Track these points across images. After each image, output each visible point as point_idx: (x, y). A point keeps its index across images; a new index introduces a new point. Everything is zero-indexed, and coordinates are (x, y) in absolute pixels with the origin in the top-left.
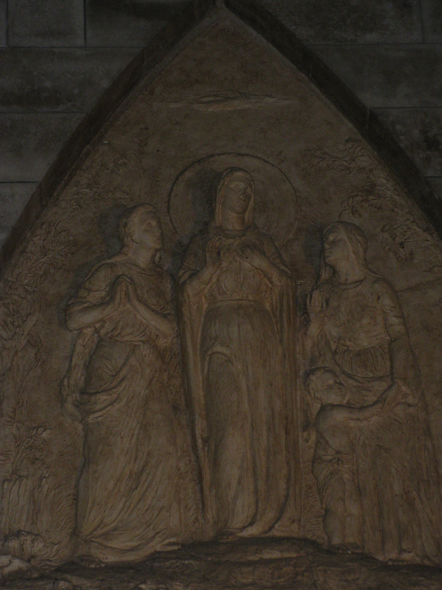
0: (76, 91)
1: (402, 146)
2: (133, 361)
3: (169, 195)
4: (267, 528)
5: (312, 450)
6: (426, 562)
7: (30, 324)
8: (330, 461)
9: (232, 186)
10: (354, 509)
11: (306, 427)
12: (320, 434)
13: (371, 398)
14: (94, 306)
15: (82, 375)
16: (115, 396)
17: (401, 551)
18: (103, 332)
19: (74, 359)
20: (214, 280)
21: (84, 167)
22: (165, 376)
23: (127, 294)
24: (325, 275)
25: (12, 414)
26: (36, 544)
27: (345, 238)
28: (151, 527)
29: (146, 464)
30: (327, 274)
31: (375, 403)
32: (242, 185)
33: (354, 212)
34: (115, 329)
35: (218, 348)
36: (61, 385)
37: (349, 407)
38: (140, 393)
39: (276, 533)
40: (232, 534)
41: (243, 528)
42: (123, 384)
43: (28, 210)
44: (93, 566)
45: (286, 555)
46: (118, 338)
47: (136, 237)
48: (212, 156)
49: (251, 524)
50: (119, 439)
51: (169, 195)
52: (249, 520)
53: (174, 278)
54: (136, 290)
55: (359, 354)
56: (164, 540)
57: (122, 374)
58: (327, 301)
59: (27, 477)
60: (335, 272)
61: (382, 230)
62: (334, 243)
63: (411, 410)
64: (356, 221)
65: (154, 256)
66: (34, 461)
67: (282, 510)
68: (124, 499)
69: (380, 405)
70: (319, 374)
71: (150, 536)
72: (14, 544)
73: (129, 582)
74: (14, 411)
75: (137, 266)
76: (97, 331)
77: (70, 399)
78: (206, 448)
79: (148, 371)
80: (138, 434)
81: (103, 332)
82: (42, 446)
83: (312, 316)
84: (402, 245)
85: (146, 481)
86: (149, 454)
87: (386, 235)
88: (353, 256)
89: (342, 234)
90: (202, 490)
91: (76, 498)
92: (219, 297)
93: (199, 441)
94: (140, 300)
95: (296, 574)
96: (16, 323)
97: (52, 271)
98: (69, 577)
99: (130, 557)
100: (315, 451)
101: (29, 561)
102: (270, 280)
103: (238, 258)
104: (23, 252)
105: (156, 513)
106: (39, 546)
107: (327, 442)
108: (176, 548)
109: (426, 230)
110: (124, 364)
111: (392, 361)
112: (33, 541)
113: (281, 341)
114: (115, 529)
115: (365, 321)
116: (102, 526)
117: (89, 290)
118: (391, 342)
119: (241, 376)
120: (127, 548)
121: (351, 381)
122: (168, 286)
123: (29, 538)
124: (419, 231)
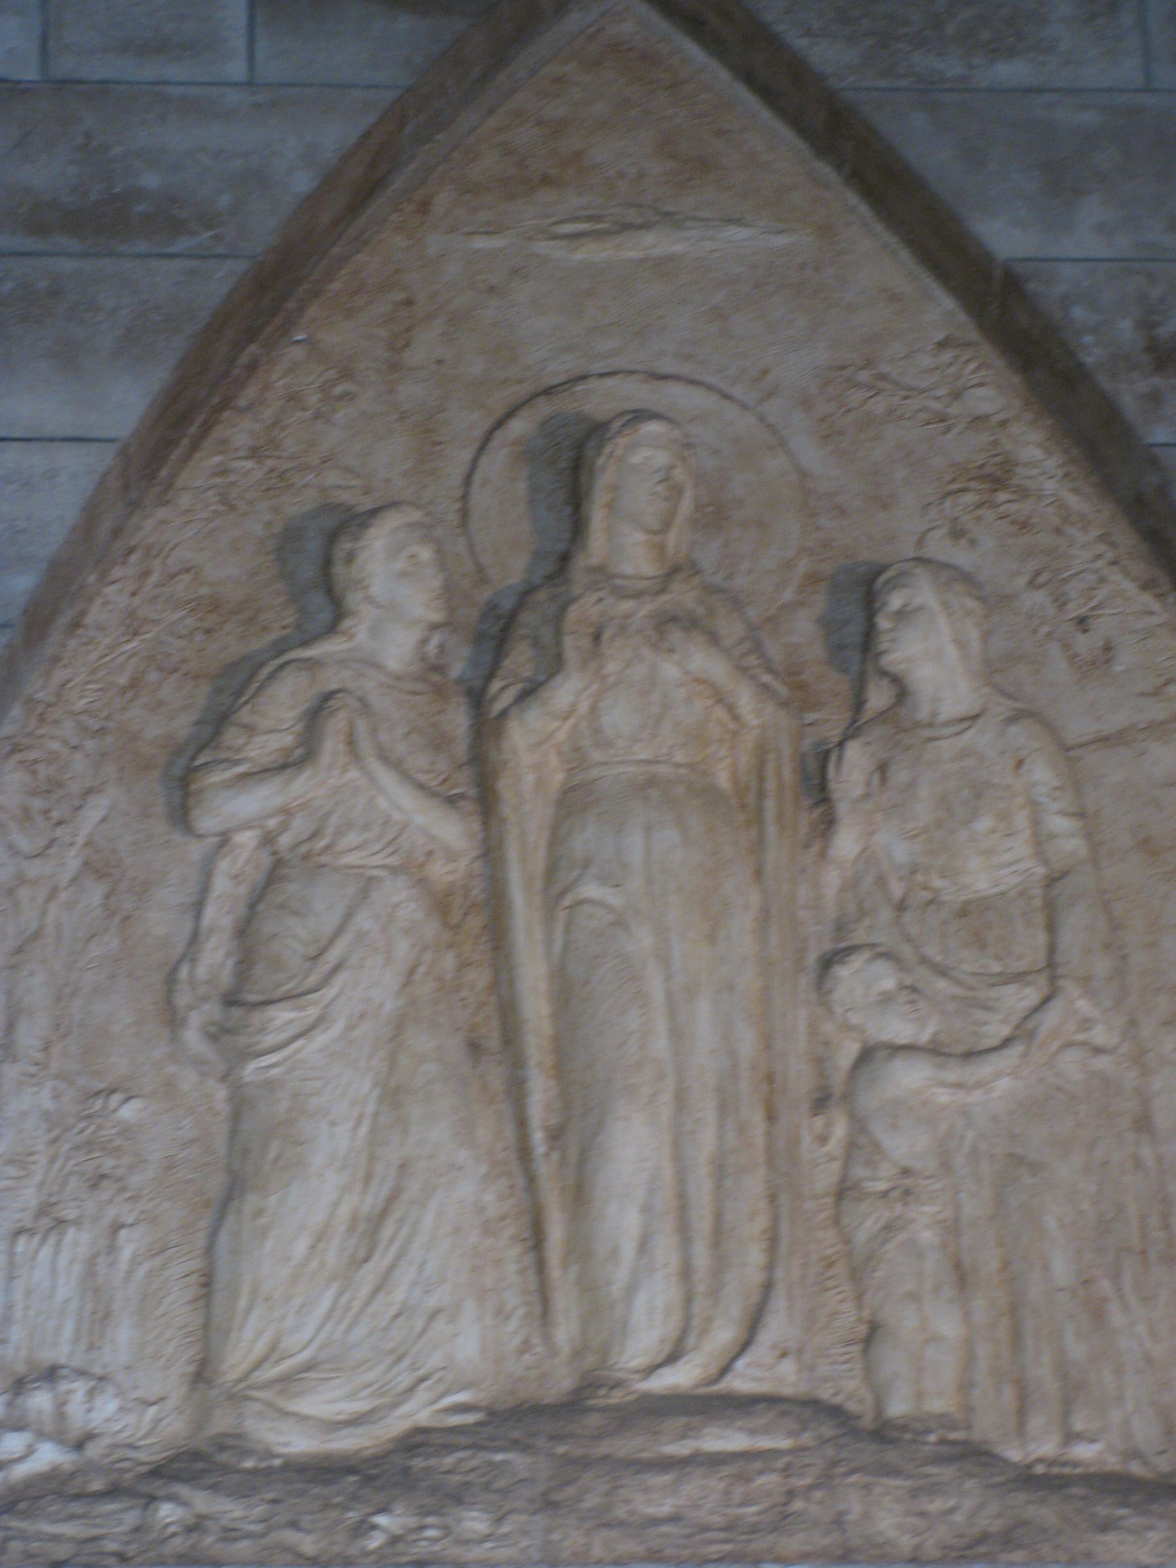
0: (224, 201)
1: (1089, 360)
2: (363, 921)
3: (468, 480)
4: (713, 1370)
5: (836, 1166)
6: (1136, 1468)
7: (92, 815)
8: (885, 1194)
9: (636, 458)
10: (949, 1325)
11: (821, 1102)
12: (859, 1124)
13: (997, 1030)
14: (265, 772)
15: (228, 955)
16: (313, 1012)
17: (1070, 1437)
18: (285, 841)
19: (210, 913)
20: (584, 707)
21: (242, 402)
22: (449, 961)
23: (351, 742)
24: (878, 697)
25: (40, 1056)
26: (98, 1402)
28: (406, 1363)
31: (1006, 1042)
32: (661, 458)
33: (957, 533)
34: (315, 835)
35: (591, 890)
36: (171, 979)
37: (935, 1050)
38: (381, 1005)
39: (741, 1382)
40: (618, 1384)
41: (651, 1370)
43: (91, 513)
44: (249, 1464)
45: (765, 1443)
46: (323, 859)
47: (378, 588)
48: (583, 378)
49: (672, 1358)
51: (468, 480)
52: (667, 1349)
53: (477, 699)
54: (374, 731)
55: (963, 912)
58: (883, 768)
59: (77, 1222)
60: (902, 690)
61: (1032, 584)
62: (902, 615)
63: (1102, 1063)
64: (962, 557)
65: (424, 641)
66: (97, 1181)
69: (1017, 1049)
70: (857, 962)
71: (401, 1388)
72: (40, 1401)
73: (347, 1509)
74: (46, 1048)
75: (378, 666)
76: (268, 839)
77: (195, 1019)
79: (403, 948)
80: (376, 1115)
81: (285, 841)
82: (118, 1142)
83: (843, 809)
84: (1082, 623)
86: (404, 1167)
88: (952, 652)
90: (541, 1267)
91: (207, 1283)
92: (597, 755)
93: (538, 1137)
94: (384, 757)
95: (791, 1494)
96: (55, 815)
97: (153, 676)
98: (183, 1490)
99: (345, 1443)
100: (846, 1167)
101: (79, 1446)
102: (731, 709)
103: (646, 652)
104: (76, 625)
105: (419, 1324)
106: (107, 1406)
107: (876, 1146)
108: (470, 1418)
109: (1147, 585)
111: (1051, 928)
112: (91, 1394)
113: (758, 873)
114: (310, 1366)
115: (984, 824)
116: (275, 1357)
117: (250, 730)
118: (1052, 881)
120: (341, 1417)
121: (942, 984)
123: (79, 1388)
124: (1129, 587)
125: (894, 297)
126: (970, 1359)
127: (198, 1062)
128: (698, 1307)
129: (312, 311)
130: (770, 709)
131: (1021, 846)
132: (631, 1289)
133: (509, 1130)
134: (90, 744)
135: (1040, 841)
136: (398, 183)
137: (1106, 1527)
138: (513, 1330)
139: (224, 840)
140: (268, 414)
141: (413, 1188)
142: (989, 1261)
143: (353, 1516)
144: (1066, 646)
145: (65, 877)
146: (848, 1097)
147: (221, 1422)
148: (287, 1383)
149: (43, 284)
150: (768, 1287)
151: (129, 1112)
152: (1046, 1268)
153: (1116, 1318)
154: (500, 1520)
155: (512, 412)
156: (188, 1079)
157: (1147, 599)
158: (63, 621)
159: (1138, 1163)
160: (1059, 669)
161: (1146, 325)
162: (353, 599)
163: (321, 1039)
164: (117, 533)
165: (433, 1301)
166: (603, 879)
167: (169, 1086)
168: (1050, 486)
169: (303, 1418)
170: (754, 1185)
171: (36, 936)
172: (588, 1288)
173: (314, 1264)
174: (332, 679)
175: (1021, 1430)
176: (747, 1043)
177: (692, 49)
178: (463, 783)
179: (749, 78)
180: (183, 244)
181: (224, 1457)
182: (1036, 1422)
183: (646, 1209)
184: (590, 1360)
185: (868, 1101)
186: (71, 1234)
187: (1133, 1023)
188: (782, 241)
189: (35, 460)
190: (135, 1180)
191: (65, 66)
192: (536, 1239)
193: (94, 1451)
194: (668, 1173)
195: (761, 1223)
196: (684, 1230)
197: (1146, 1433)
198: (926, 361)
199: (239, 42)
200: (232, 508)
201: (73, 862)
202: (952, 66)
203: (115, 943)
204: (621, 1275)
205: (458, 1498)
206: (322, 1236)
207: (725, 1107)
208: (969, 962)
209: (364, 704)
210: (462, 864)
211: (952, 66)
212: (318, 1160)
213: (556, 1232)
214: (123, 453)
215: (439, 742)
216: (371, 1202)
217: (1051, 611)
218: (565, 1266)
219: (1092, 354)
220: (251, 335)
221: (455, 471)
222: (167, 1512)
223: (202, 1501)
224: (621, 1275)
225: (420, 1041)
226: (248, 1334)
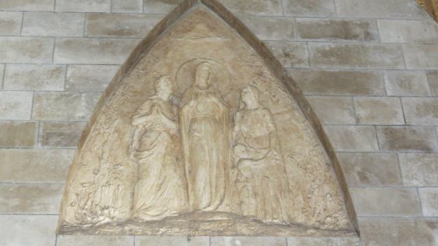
2: (159, 139)
6: (284, 224)
7: (116, 123)
8: (244, 181)
11: (233, 167)
13: (261, 156)
18: (147, 126)
22: (173, 146)
23: (157, 111)
24: (242, 107)
27: (250, 90)
29: (164, 180)
32: (207, 68)
37: (251, 159)
39: (220, 209)
41: (205, 208)
42: (155, 148)
43: (117, 76)
47: (162, 88)
49: (209, 206)
53: (178, 106)
54: (161, 110)
55: (255, 139)
57: (155, 144)
58: (242, 117)
59: (113, 184)
62: (246, 93)
63: (278, 162)
65: (169, 97)
66: (116, 178)
67: (222, 201)
72: (106, 211)
74: (108, 158)
76: (144, 126)
77: (132, 154)
79: (165, 143)
81: (147, 126)
84: (274, 96)
86: (165, 177)
87: (267, 92)
88: (254, 99)
89: (249, 89)
90: (188, 192)
91: (133, 194)
94: (162, 113)
97: (126, 102)
99: (155, 219)
102: (218, 106)
104: (114, 95)
106: (117, 213)
107: (242, 174)
109: (284, 91)
110: (156, 140)
113: (223, 132)
115: (259, 125)
118: (269, 134)
121: (252, 150)
122: (175, 109)
123: (113, 209)
124: (281, 91)
125: (243, 48)
126: (257, 207)
127: (132, 160)
128: (213, 198)
129: (152, 49)
130: (224, 107)
131: (264, 129)
132: (202, 195)
133: (183, 171)
134: (116, 112)
135: (267, 127)
136: (166, 31)
137: (280, 231)
138: (183, 202)
139: (137, 126)
140: (145, 64)
141: (167, 180)
142: (260, 193)
143: (157, 229)
144: (271, 99)
146: (237, 167)
147: (135, 215)
150: (224, 195)
151: (121, 168)
152: (269, 192)
153: (281, 200)
154: (181, 229)
155: (184, 64)
156: (131, 163)
157: (284, 93)
158: (112, 93)
159: (284, 177)
160: (270, 103)
161: (284, 51)
162: (158, 89)
163: (152, 156)
164: (121, 81)
166: (198, 132)
167: (128, 164)
169: (149, 215)
170: (222, 179)
171: (107, 141)
172: (195, 195)
174: (155, 101)
175: (266, 218)
176: (221, 158)
177: (212, 12)
178: (176, 118)
179: (221, 16)
180: (132, 36)
181: (135, 220)
182: (268, 217)
184: (196, 206)
185: (240, 167)
186: (111, 186)
187: (283, 156)
188: (226, 40)
189: (108, 68)
190: (123, 178)
191: (114, 11)
192: (187, 188)
193: (115, 219)
195: (223, 185)
196: (211, 186)
197: (285, 218)
198: (248, 58)
199: (141, 7)
200: (139, 77)
201: (113, 130)
202: (253, 13)
204: (201, 193)
205: (173, 226)
206: (153, 186)
207: (218, 167)
208: (257, 146)
209: (160, 106)
210: (175, 131)
211: (253, 13)
214: (122, 67)
215: (172, 112)
216: (160, 182)
217: (269, 94)
219: (275, 54)
220: (143, 52)
221: (175, 73)
222: (127, 228)
223: (132, 227)
224: (201, 193)
225: (169, 158)
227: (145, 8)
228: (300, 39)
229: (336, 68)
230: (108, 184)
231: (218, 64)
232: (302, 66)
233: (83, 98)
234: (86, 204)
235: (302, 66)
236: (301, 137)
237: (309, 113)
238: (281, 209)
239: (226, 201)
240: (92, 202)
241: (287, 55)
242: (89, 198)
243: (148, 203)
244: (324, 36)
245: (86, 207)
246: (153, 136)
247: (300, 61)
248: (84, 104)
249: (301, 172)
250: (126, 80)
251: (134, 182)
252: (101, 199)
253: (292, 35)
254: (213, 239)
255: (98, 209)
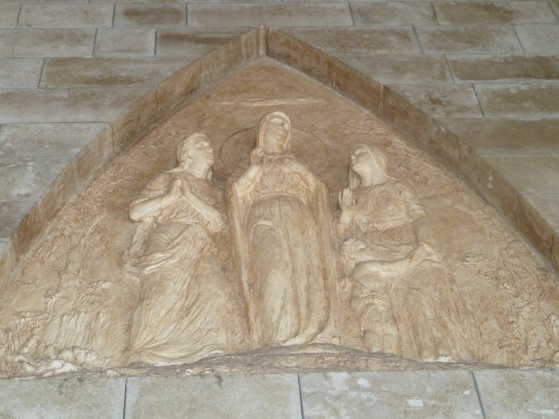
1: (412, 103)
4: (309, 339)
9: (273, 121)
11: (342, 277)
16: (168, 255)
17: (438, 356)
19: (135, 239)
25: (76, 273)
26: (89, 356)
28: (200, 342)
29: (196, 301)
30: (354, 185)
35: (262, 222)
38: (192, 256)
42: (177, 248)
46: (174, 220)
49: (295, 336)
50: (172, 283)
56: (211, 351)
57: (176, 242)
67: (321, 329)
68: (174, 324)
71: (198, 348)
74: (78, 271)
78: (252, 290)
79: (199, 243)
80: (189, 283)
82: (101, 293)
85: (195, 311)
91: (129, 327)
93: (245, 285)
105: (205, 333)
112: (86, 354)
115: (390, 208)
116: (152, 342)
117: (150, 190)
119: (282, 239)
120: (176, 357)
123: (83, 353)
126: (400, 339)
131: (403, 215)
132: (279, 320)
133: (236, 289)
135: (409, 213)
138: (238, 338)
141: (202, 299)
145: (88, 233)
148: (157, 348)
149: (89, 93)
151: (105, 286)
153: (451, 326)
163: (171, 261)
165: (209, 327)
166: (265, 219)
168: (403, 147)
173: (168, 317)
176: (316, 261)
182: (425, 353)
183: (284, 298)
184: (265, 340)
185: (357, 275)
192: (246, 315)
194: (290, 290)
196: (296, 302)
203: (104, 248)
204: (275, 316)
207: (309, 273)
212: (169, 291)
213: (252, 310)
218: (255, 318)
224: (275, 316)
226: (144, 335)
227: (158, 50)
228: (457, 81)
229: (537, 116)
230: (76, 311)
231: (302, 132)
232: (468, 115)
233: (30, 169)
234: (24, 346)
235: (468, 115)
236: (481, 230)
237: (490, 186)
238: (453, 340)
239: (330, 329)
240: (39, 343)
241: (435, 102)
242: (32, 335)
243: (162, 338)
244: (504, 76)
245: (26, 350)
246: (173, 231)
247: (462, 109)
248: (32, 176)
249: (488, 282)
250: (121, 159)
251: (131, 308)
252: (58, 336)
253: (443, 76)
254: (305, 379)
255: (51, 351)
